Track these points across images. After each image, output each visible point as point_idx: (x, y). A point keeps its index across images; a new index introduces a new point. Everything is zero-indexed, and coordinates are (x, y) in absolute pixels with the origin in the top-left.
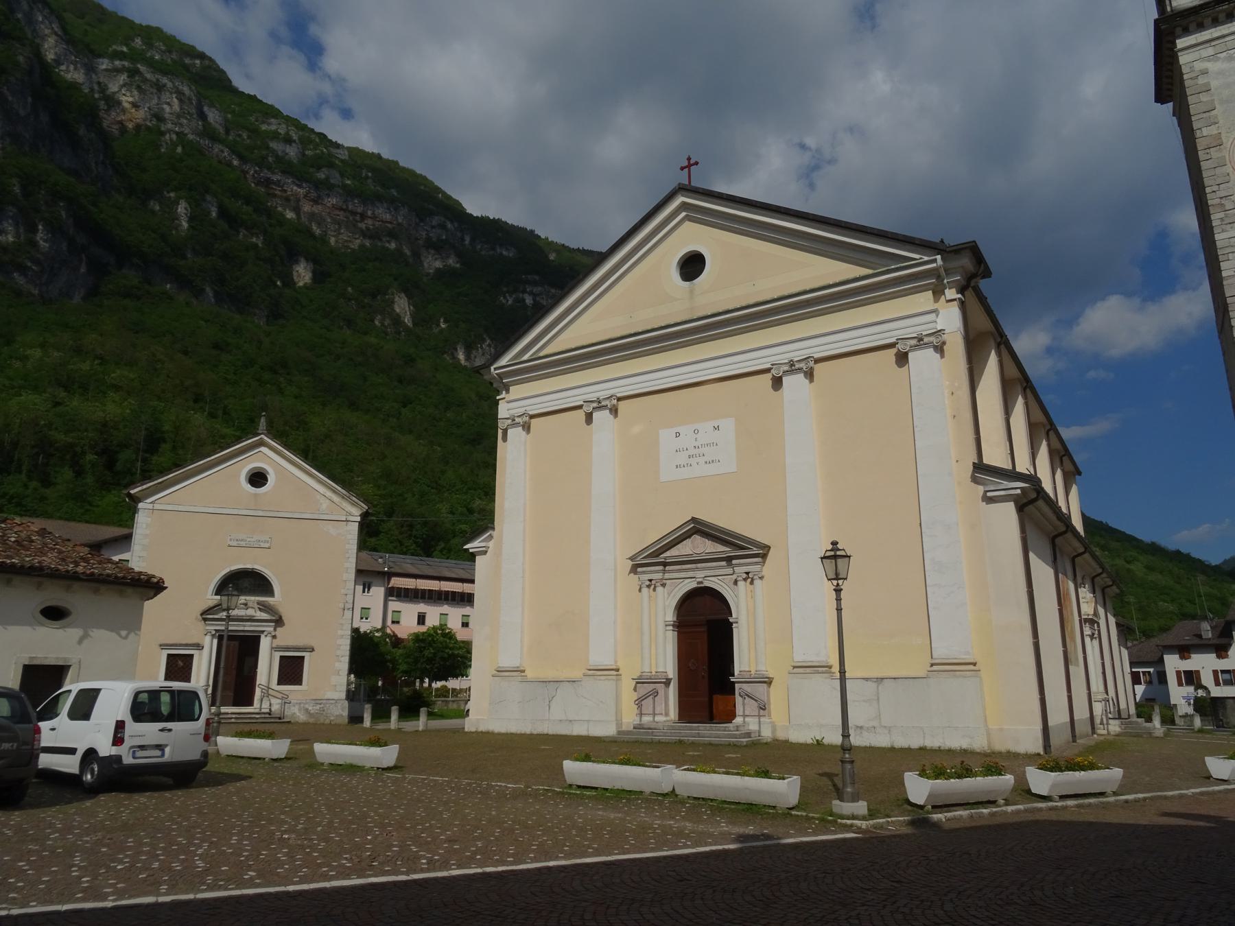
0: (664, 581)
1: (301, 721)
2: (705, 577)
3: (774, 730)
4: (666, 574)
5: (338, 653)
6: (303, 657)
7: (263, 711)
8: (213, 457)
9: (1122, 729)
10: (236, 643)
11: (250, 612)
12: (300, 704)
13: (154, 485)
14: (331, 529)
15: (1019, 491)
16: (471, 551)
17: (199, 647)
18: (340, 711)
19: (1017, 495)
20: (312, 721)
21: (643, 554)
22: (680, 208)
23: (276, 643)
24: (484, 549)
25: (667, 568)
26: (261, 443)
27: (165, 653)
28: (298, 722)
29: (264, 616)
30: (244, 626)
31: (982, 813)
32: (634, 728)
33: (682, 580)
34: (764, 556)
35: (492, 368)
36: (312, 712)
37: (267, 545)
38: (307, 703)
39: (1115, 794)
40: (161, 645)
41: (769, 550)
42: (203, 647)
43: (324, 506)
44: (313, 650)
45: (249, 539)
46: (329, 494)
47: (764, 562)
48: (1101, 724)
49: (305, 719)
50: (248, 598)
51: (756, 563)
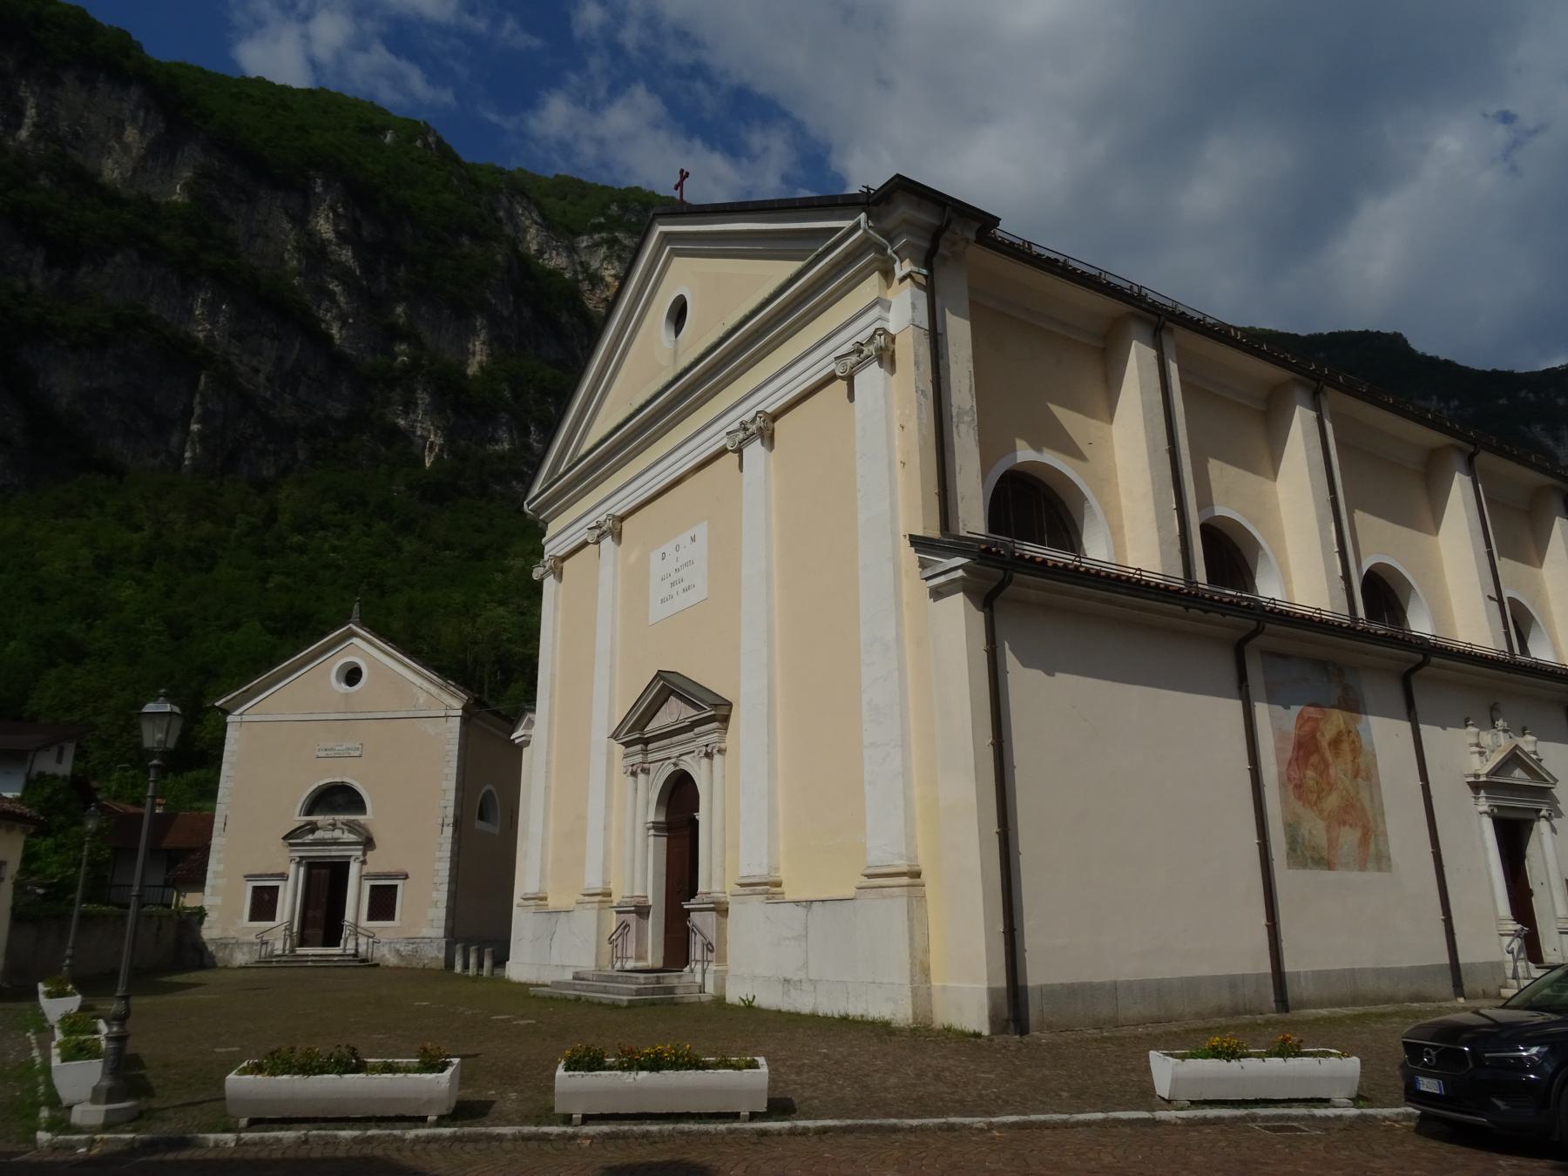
0: (646, 766)
1: (391, 965)
2: (681, 755)
3: (721, 982)
4: (649, 755)
5: (437, 879)
6: (396, 886)
7: (348, 952)
8: (298, 656)
9: (1553, 991)
10: (325, 872)
11: (337, 834)
12: (390, 943)
13: (239, 694)
14: (429, 727)
15: (960, 573)
16: (517, 741)
17: (283, 876)
18: (436, 952)
19: (962, 578)
20: (403, 964)
21: (622, 729)
22: (661, 244)
23: (367, 869)
24: (523, 738)
25: (651, 746)
26: (355, 635)
27: (251, 885)
28: (387, 966)
29: (352, 838)
30: (330, 850)
31: (336, 1137)
32: (574, 978)
33: (661, 763)
34: (725, 719)
35: (525, 505)
36: (404, 953)
37: (357, 753)
38: (397, 943)
39: (754, 1116)
40: (246, 877)
41: (731, 709)
42: (288, 877)
43: (421, 700)
44: (406, 877)
45: (337, 748)
46: (426, 685)
47: (726, 729)
48: (1513, 978)
49: (396, 962)
50: (337, 817)
51: (713, 731)
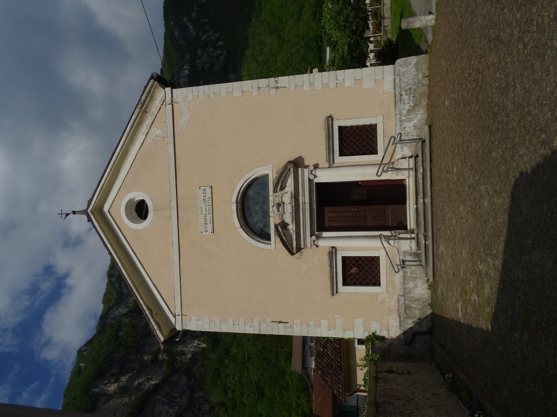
1: (425, 116)
5: (332, 85)
7: (412, 165)
11: (287, 199)
12: (401, 121)
13: (153, 317)
20: (424, 102)
23: (323, 163)
29: (290, 182)
30: (304, 203)
36: (412, 104)
37: (208, 190)
38: (400, 113)
40: (333, 294)
42: (333, 247)
43: (158, 132)
45: (204, 212)
46: (144, 129)
50: (271, 204)
